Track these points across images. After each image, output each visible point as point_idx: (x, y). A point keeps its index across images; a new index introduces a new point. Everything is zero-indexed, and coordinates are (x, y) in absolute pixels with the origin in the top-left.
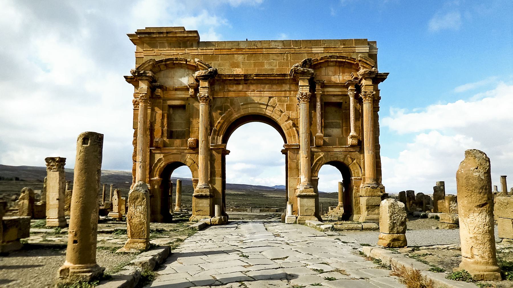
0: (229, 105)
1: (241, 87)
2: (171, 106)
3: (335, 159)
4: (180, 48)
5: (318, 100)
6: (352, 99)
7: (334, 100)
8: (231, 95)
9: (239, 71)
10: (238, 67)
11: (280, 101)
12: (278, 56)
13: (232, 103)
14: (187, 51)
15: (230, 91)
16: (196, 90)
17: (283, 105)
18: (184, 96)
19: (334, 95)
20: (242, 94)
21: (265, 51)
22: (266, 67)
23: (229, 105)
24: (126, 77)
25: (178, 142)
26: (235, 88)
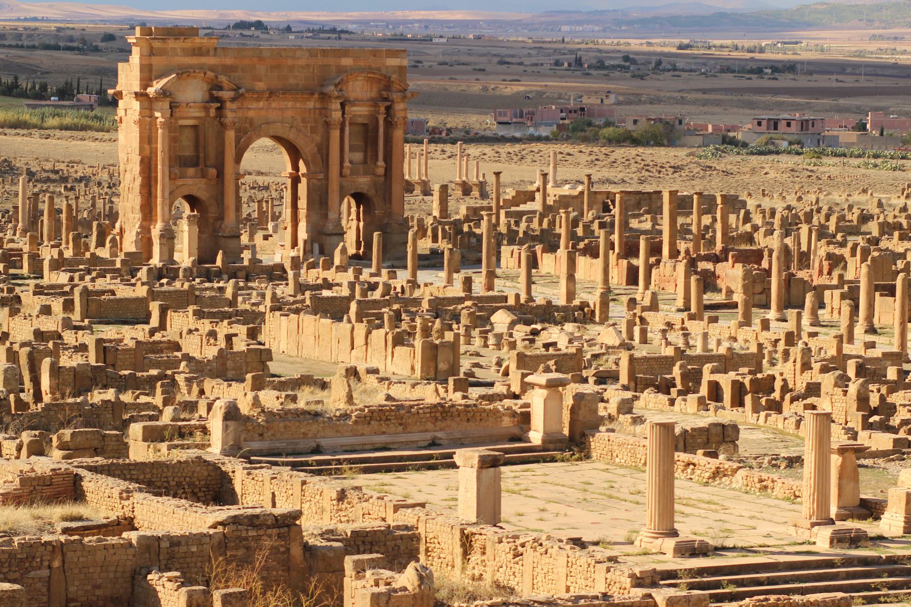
0: (248, 125)
1: (261, 104)
2: (180, 126)
3: (359, 191)
4: (195, 55)
5: (347, 124)
6: (381, 122)
7: (360, 120)
8: (251, 114)
9: (261, 86)
10: (261, 81)
11: (304, 121)
12: (303, 68)
13: (251, 124)
14: (204, 60)
15: (250, 109)
16: (220, 109)
17: (306, 127)
18: (198, 115)
19: (360, 116)
20: (263, 113)
21: (290, 62)
22: (292, 81)
23: (248, 125)
24: (136, 93)
25: (191, 171)
26: (255, 105)
